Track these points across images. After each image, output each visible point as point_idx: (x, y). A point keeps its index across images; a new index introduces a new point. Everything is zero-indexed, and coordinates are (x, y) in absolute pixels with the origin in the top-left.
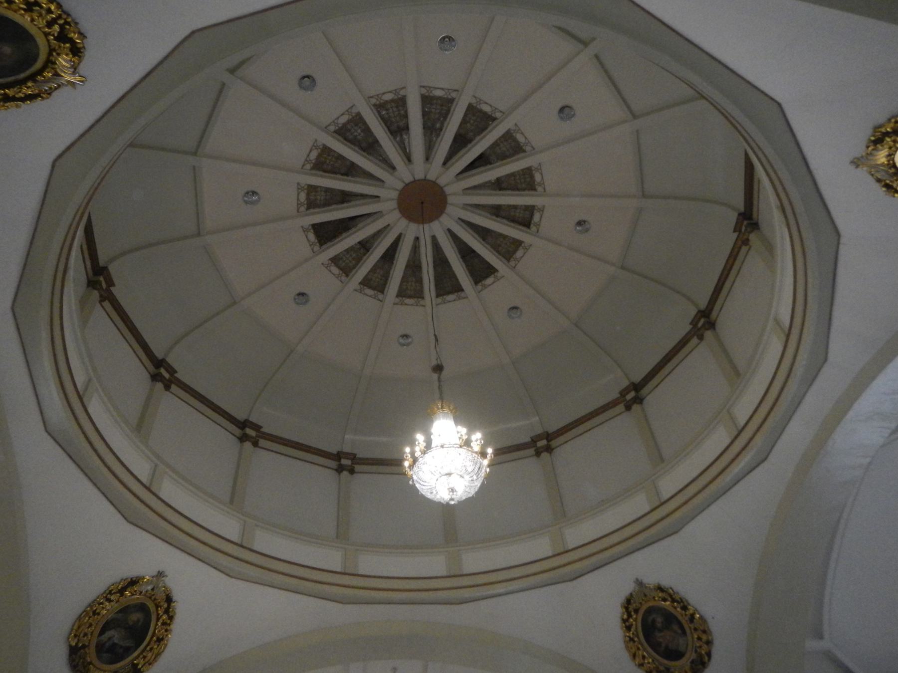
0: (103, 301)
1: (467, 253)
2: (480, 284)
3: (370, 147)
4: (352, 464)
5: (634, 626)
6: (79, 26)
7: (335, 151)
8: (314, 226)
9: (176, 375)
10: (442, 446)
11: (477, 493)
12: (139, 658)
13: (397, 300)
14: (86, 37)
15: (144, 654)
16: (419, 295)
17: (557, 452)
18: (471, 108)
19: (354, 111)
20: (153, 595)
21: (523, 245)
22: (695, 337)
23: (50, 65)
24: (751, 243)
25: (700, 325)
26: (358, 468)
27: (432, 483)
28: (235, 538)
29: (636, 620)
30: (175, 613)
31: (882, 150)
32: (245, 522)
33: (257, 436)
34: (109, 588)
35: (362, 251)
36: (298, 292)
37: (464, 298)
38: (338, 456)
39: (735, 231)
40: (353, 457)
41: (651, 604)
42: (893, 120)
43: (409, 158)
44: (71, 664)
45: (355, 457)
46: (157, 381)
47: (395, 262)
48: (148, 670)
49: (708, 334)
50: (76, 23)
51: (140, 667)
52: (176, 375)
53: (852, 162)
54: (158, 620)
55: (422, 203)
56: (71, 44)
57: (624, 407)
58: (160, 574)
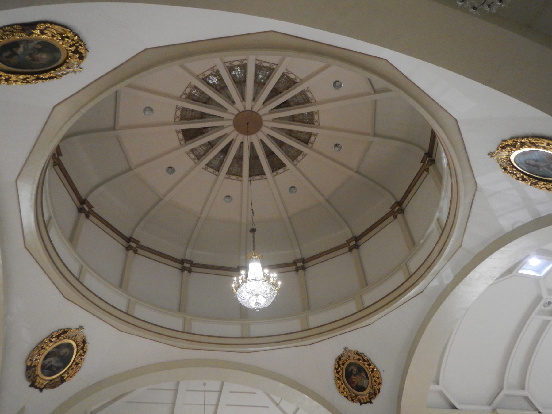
1: (269, 154)
2: (275, 172)
4: (190, 266)
5: (341, 372)
6: (86, 46)
8: (183, 130)
9: (92, 209)
10: (255, 280)
11: (270, 305)
13: (227, 176)
14: (88, 51)
15: (68, 371)
16: (239, 174)
18: (283, 75)
20: (76, 339)
21: (303, 153)
24: (429, 171)
25: (395, 210)
26: (193, 269)
27: (247, 297)
28: (124, 309)
29: (342, 369)
30: (87, 350)
31: (504, 152)
33: (136, 247)
34: (51, 334)
35: (209, 146)
38: (182, 262)
40: (191, 263)
41: (352, 361)
42: (512, 140)
43: (243, 99)
44: (27, 376)
45: (192, 263)
46: (82, 212)
47: (227, 155)
48: (69, 380)
50: (85, 45)
51: (65, 378)
52: (92, 209)
53: (489, 154)
54: (77, 352)
55: (248, 124)
56: (80, 55)
57: (348, 249)
58: (81, 327)
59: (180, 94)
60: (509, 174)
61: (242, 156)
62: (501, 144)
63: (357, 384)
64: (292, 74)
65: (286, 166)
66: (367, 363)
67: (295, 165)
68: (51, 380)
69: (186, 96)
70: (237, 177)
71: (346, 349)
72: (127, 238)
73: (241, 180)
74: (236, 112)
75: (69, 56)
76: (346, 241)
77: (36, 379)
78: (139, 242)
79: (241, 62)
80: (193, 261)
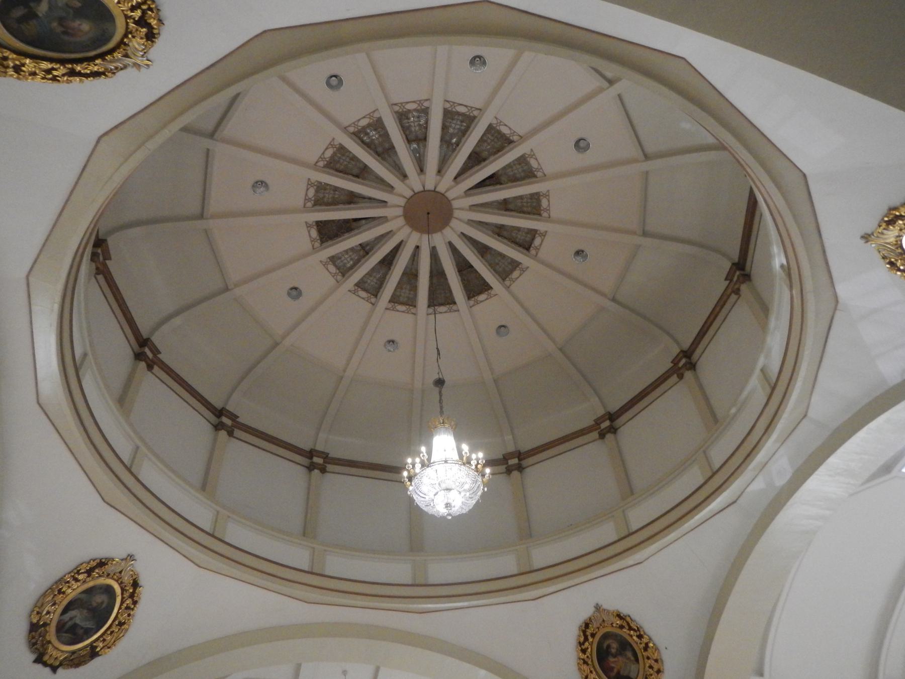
0: (97, 274)
1: (464, 267)
2: (473, 299)
4: (324, 462)
5: (589, 650)
7: (350, 152)
9: (159, 356)
10: (446, 462)
11: (470, 511)
12: (99, 641)
13: (390, 306)
14: (163, 24)
15: (104, 637)
16: (411, 303)
18: (490, 128)
19: (376, 115)
20: (121, 578)
21: (520, 266)
22: (675, 376)
23: (122, 46)
24: (741, 293)
25: (681, 364)
26: (330, 467)
28: (207, 528)
29: (591, 644)
31: (892, 231)
32: (218, 512)
35: (362, 253)
36: (292, 286)
38: (311, 454)
39: (726, 279)
40: (325, 456)
41: (609, 629)
43: (422, 170)
45: (327, 456)
46: (141, 360)
47: (392, 268)
48: (105, 653)
49: (688, 375)
51: (98, 649)
52: (159, 356)
53: (862, 237)
54: (122, 602)
55: (428, 213)
56: (148, 30)
58: (131, 557)
59: (315, 160)
60: (899, 273)
61: (417, 271)
62: (886, 216)
63: (618, 673)
64: (505, 127)
65: (491, 288)
66: (635, 634)
67: (508, 288)
68: (73, 653)
69: (325, 163)
70: (408, 307)
71: (598, 608)
73: (414, 312)
74: (409, 193)
75: (129, 30)
76: (594, 421)
77: (46, 649)
78: (238, 417)
79: (419, 104)
80: (329, 454)
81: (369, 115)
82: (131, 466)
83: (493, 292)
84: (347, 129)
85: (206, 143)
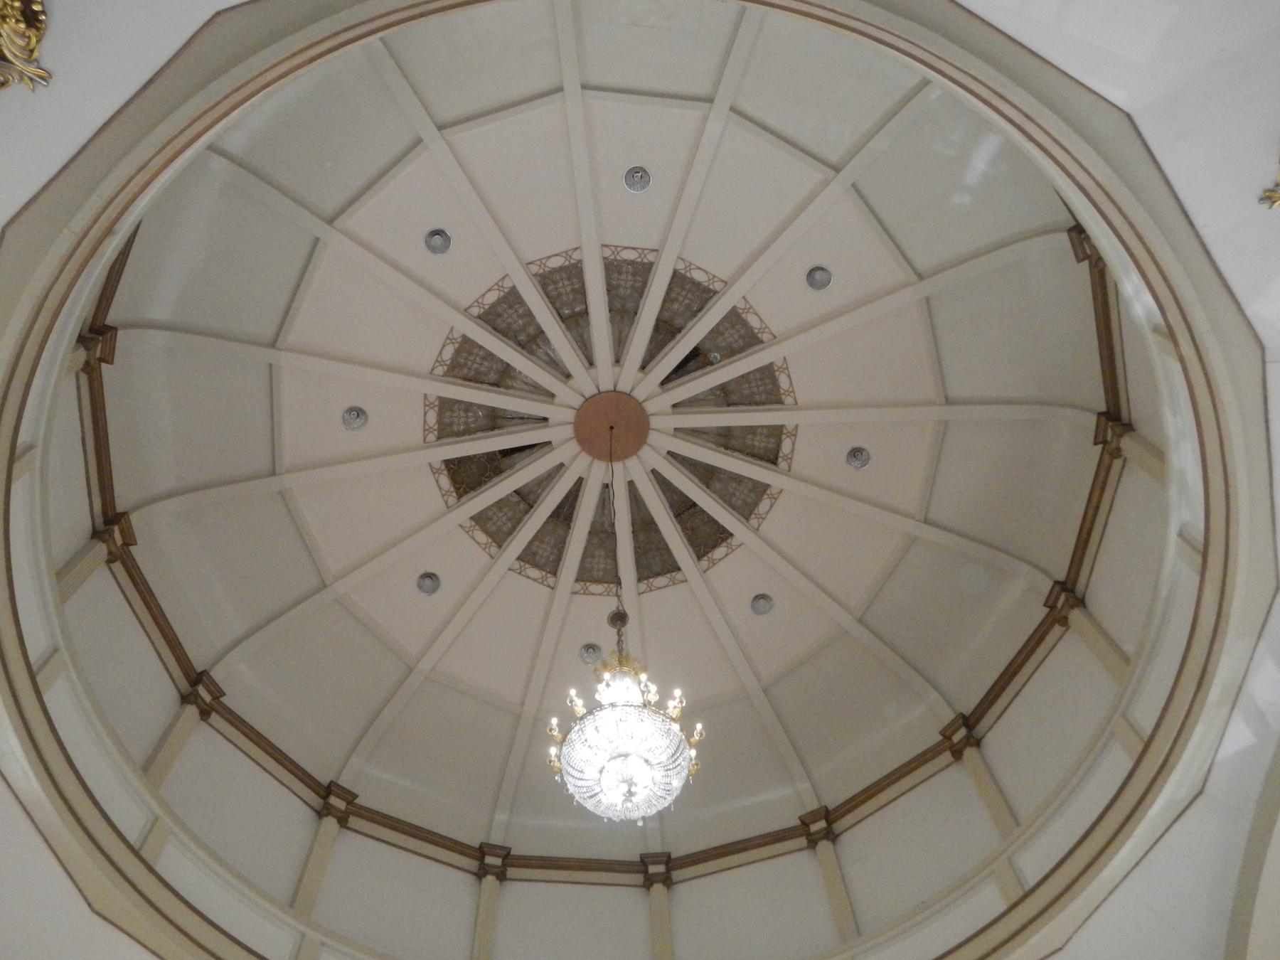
1: (683, 508)
3: (532, 341)
7: (481, 347)
8: (448, 463)
17: (845, 839)
19: (507, 284)
24: (1125, 453)
25: (1059, 605)
35: (522, 506)
36: (422, 571)
37: (682, 582)
47: (572, 525)
53: (1262, 199)
65: (731, 535)
70: (606, 585)
72: (319, 784)
81: (498, 285)
82: (141, 848)
83: (734, 542)
84: (468, 311)
85: (268, 355)
